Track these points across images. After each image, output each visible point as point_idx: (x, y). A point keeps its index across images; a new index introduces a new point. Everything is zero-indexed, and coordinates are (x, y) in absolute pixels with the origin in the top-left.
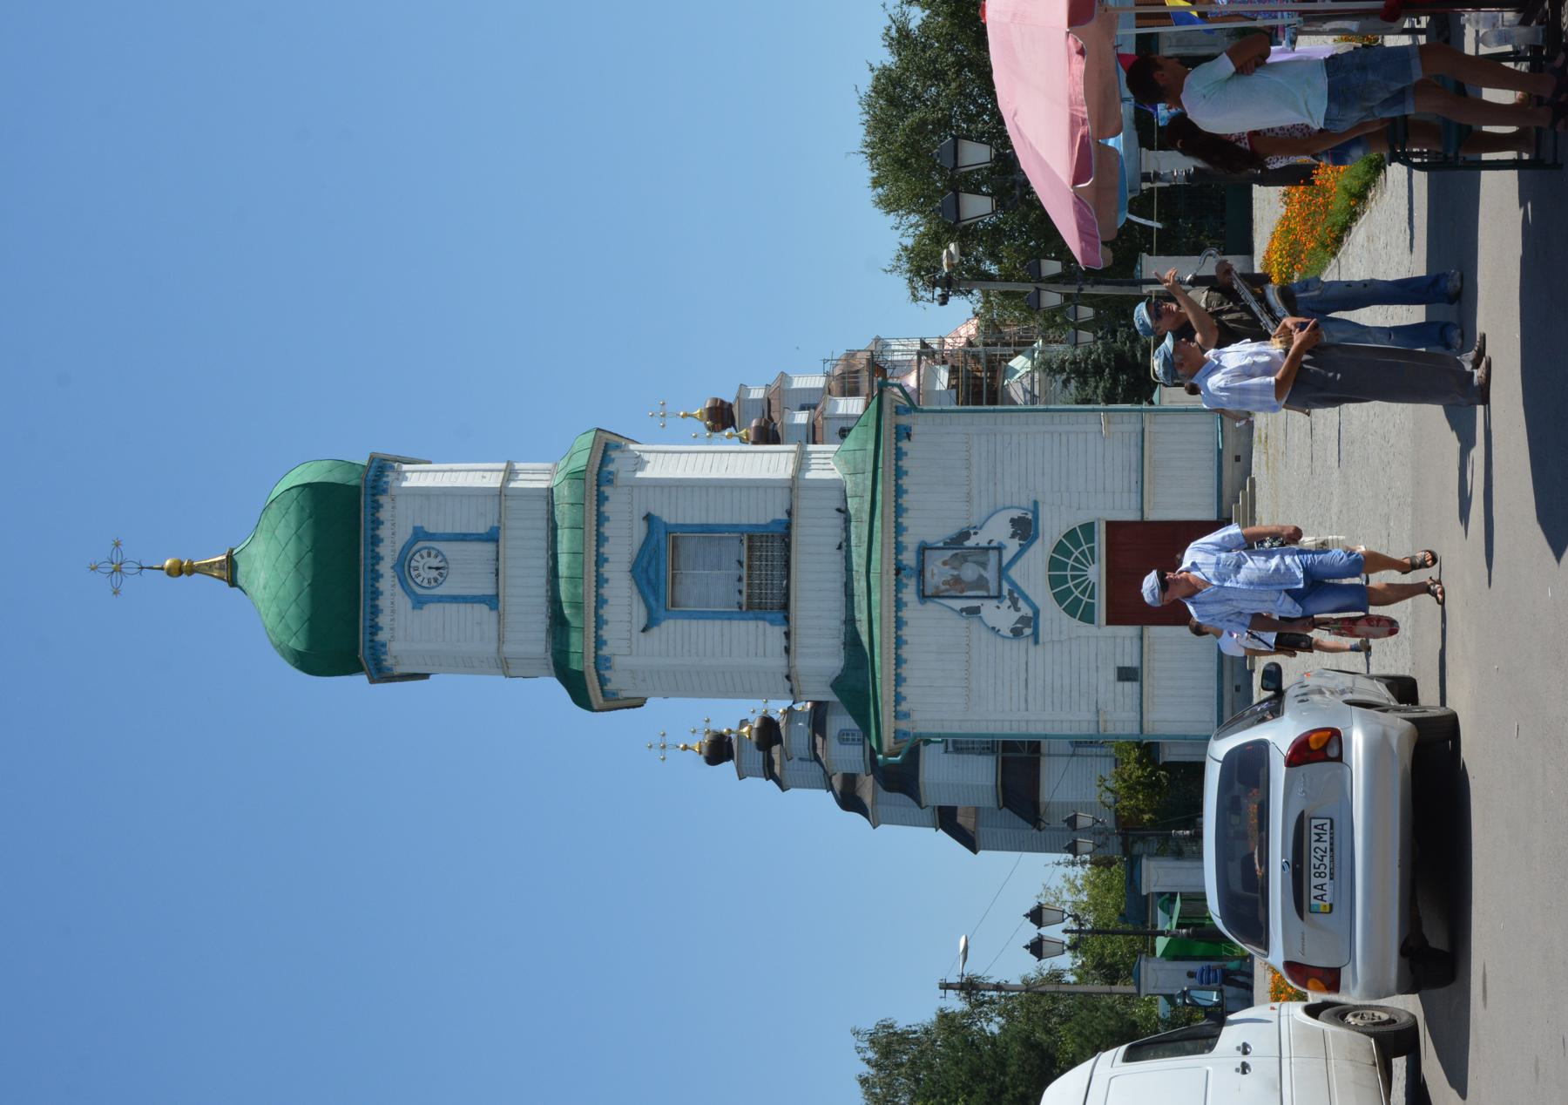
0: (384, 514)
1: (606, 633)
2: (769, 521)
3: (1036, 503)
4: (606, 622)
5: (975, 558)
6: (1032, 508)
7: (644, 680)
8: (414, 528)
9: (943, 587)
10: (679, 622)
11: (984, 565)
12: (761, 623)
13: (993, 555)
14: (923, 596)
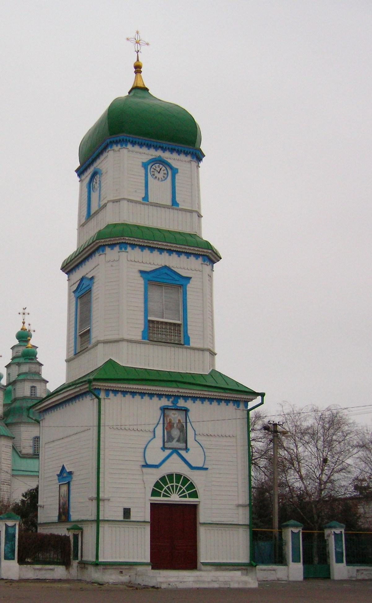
0: (182, 157)
1: (137, 250)
2: (189, 335)
3: (207, 469)
4: (142, 251)
5: (181, 437)
6: (205, 467)
7: (112, 266)
8: (177, 169)
9: (168, 419)
10: (143, 286)
11: (178, 441)
12: (143, 326)
13: (182, 445)
14: (164, 409)
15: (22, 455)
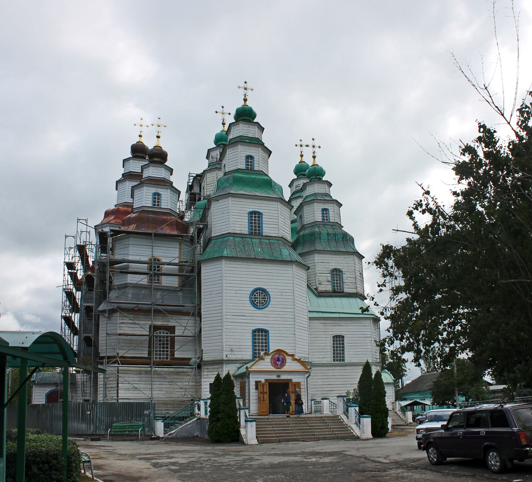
15: (318, 293)
